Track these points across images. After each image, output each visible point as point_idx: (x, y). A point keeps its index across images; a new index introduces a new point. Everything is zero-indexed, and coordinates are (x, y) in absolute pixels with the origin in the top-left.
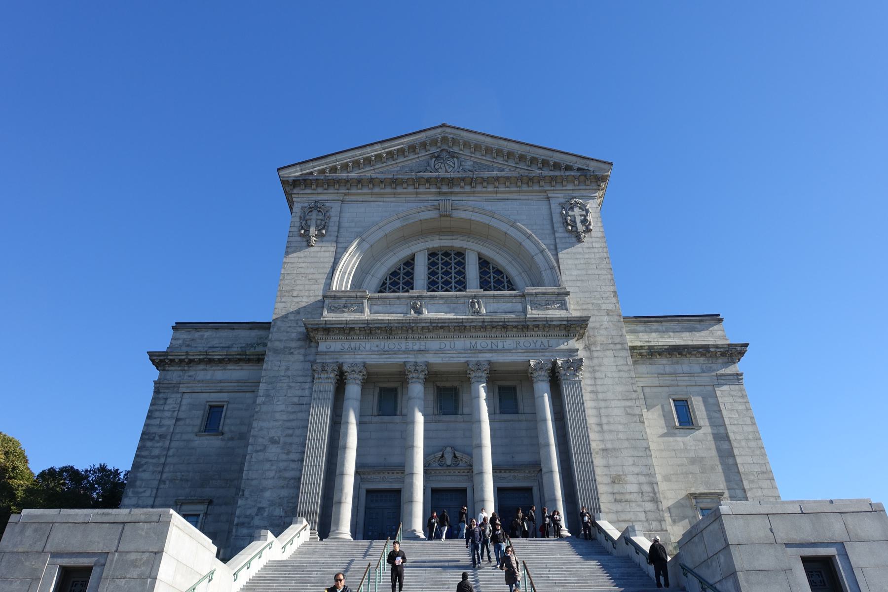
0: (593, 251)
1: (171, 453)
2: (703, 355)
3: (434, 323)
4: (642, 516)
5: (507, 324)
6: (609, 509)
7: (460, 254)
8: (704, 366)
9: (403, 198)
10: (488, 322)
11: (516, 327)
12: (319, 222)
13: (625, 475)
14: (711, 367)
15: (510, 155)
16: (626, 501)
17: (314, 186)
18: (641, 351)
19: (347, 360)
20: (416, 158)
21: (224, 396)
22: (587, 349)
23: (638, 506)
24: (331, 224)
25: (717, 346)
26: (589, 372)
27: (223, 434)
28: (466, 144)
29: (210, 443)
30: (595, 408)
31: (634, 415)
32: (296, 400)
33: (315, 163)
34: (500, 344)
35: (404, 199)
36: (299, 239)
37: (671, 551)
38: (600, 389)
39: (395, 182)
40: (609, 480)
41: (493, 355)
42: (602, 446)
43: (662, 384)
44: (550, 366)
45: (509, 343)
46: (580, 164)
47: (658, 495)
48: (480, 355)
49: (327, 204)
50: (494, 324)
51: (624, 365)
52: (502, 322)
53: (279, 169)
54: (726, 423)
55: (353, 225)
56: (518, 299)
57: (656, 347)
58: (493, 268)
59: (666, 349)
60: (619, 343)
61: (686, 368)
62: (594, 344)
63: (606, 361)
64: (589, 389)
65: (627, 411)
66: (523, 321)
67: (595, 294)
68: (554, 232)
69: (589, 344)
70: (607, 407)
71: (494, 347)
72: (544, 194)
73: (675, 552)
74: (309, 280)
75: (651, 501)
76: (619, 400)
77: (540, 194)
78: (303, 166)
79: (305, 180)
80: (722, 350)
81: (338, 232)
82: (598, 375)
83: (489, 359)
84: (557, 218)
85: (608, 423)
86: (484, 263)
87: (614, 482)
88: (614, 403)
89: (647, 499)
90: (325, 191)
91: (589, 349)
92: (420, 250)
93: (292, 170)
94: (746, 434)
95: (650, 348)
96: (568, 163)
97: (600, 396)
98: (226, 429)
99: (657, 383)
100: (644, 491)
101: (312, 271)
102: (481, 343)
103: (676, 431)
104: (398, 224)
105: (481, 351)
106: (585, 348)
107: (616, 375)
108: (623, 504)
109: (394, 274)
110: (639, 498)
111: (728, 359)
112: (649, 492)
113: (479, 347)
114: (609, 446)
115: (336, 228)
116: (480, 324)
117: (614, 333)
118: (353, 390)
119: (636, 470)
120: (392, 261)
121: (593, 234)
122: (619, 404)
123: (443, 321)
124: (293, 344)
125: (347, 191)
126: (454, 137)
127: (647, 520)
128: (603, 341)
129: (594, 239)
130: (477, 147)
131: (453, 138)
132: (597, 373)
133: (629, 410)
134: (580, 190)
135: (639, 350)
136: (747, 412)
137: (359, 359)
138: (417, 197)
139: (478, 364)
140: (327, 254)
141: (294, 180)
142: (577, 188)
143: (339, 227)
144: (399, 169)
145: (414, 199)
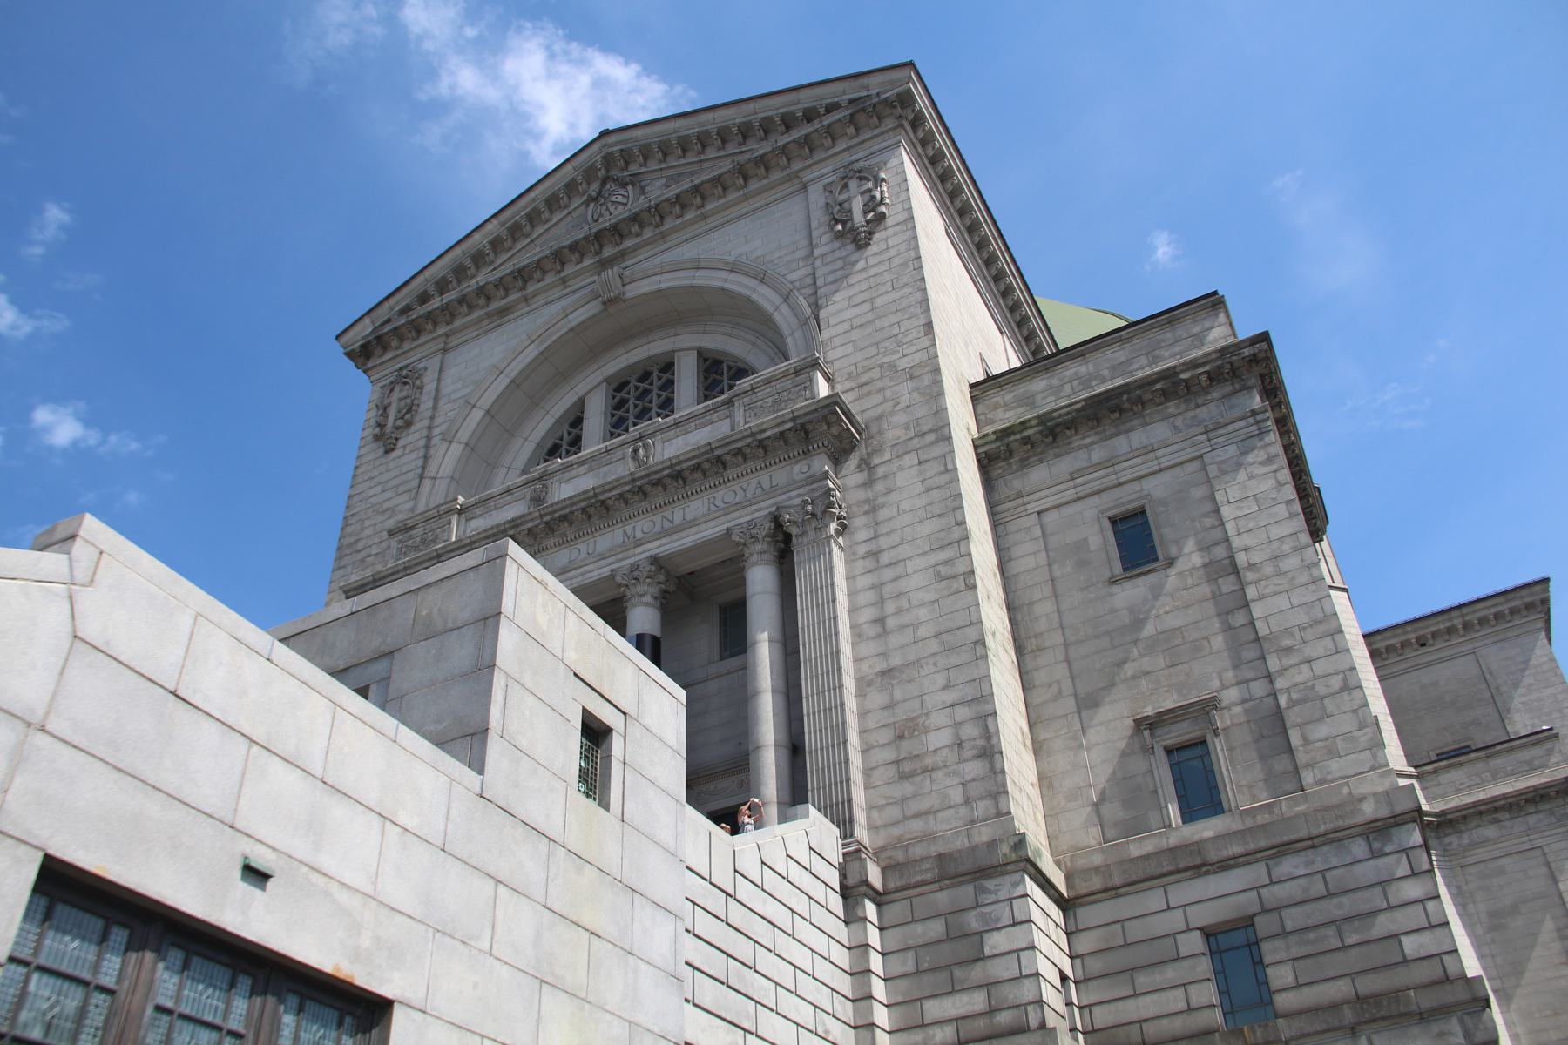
0: (887, 255)
2: (1166, 395)
3: (546, 514)
4: (957, 796)
5: (678, 468)
6: (886, 798)
8: (1179, 422)
9: (541, 299)
10: (642, 478)
11: (697, 468)
12: (403, 403)
13: (927, 714)
14: (1194, 417)
16: (923, 772)
17: (394, 343)
18: (1026, 433)
20: (565, 216)
22: (863, 466)
23: (947, 775)
25: (1194, 364)
26: (866, 513)
30: (873, 587)
31: (955, 577)
33: (392, 301)
34: (677, 515)
35: (543, 302)
36: (374, 446)
37: (1005, 855)
39: (522, 276)
40: (885, 736)
41: (664, 540)
42: (882, 665)
43: (1082, 491)
44: (769, 525)
46: (852, 91)
47: (994, 741)
48: (638, 550)
49: (421, 366)
50: (652, 478)
51: (942, 473)
52: (666, 468)
53: (338, 337)
54: (1230, 535)
56: (723, 412)
57: (1055, 414)
58: (730, 368)
59: (1078, 410)
60: (930, 431)
61: (1138, 437)
62: (879, 451)
63: (901, 479)
65: (939, 573)
66: (706, 453)
67: (887, 344)
68: (812, 247)
69: (868, 454)
71: (667, 525)
72: (796, 181)
73: (1014, 855)
75: (980, 756)
76: (924, 554)
77: (786, 185)
79: (379, 338)
80: (1207, 368)
81: (435, 408)
82: (883, 514)
83: (654, 552)
84: (819, 217)
85: (899, 611)
87: (901, 737)
89: (974, 752)
90: (416, 343)
91: (868, 465)
93: (357, 329)
94: (1277, 544)
95: (1043, 419)
96: (829, 101)
97: (885, 558)
99: (1071, 494)
100: (964, 738)
103: (1115, 589)
104: (532, 353)
106: (859, 466)
107: (924, 500)
108: (917, 779)
110: (952, 757)
111: (1233, 384)
112: (975, 739)
113: (639, 535)
114: (896, 660)
115: (430, 404)
116: (627, 488)
117: (921, 412)
119: (949, 697)
120: (541, 426)
121: (889, 221)
122: (920, 562)
123: (560, 506)
125: (449, 328)
126: (623, 147)
127: (967, 802)
128: (899, 438)
129: (890, 231)
131: (622, 150)
132: (881, 511)
133: (944, 570)
134: (863, 142)
135: (1021, 432)
136: (1278, 492)
138: (566, 287)
139: (635, 567)
141: (362, 346)
142: (856, 141)
143: (436, 399)
145: (565, 292)
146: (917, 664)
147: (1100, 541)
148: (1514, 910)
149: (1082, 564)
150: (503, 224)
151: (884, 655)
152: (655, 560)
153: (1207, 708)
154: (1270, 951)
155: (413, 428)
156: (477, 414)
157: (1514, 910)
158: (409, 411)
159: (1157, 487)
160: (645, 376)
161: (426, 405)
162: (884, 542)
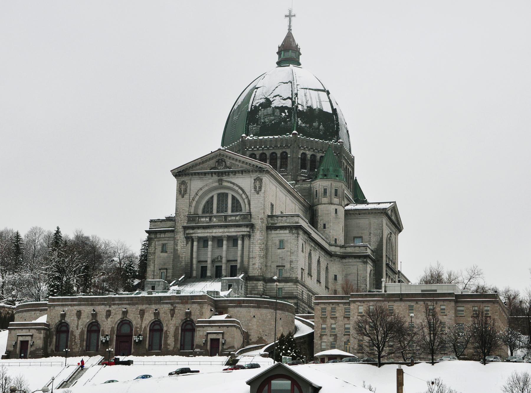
1: (156, 257)
7: (227, 194)
15: (240, 161)
19: (194, 235)
21: (166, 242)
24: (188, 189)
27: (167, 252)
28: (227, 156)
29: (164, 255)
31: (261, 248)
32: (183, 245)
33: (181, 168)
38: (254, 241)
45: (232, 230)
49: (186, 181)
53: (171, 171)
55: (194, 189)
64: (252, 241)
68: (251, 190)
70: (255, 246)
74: (183, 210)
78: (178, 169)
82: (255, 237)
84: (253, 185)
86: (233, 198)
88: (257, 245)
92: (215, 194)
97: (254, 243)
98: (168, 251)
99: (276, 236)
101: (183, 206)
102: (226, 230)
105: (226, 232)
109: (207, 202)
118: (195, 244)
119: (258, 262)
120: (207, 198)
121: (263, 191)
122: (258, 245)
124: (181, 230)
130: (230, 158)
137: (196, 235)
139: (225, 236)
140: (187, 200)
144: (207, 166)
146: (255, 257)
147: (278, 243)
148: (350, 274)
149: (275, 245)
150: (202, 160)
151: (252, 255)
152: (228, 236)
153: (284, 266)
154: (283, 291)
155: (187, 195)
156: (198, 197)
157: (350, 274)
158: (186, 191)
159: (285, 239)
160: (223, 194)
161: (188, 191)
162: (254, 241)
